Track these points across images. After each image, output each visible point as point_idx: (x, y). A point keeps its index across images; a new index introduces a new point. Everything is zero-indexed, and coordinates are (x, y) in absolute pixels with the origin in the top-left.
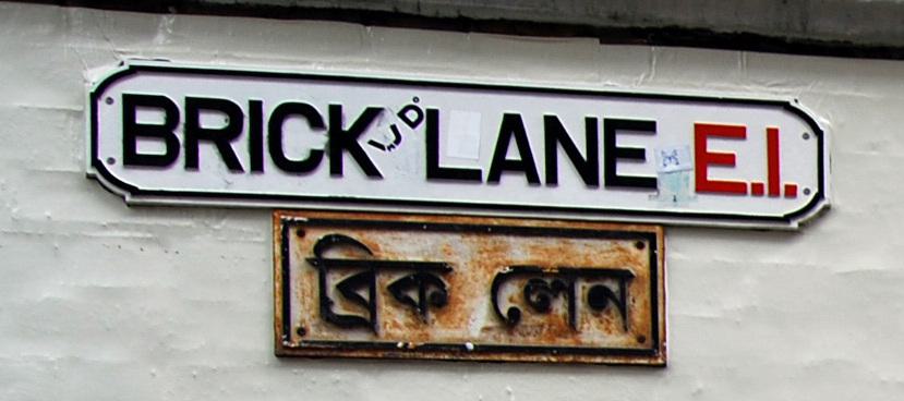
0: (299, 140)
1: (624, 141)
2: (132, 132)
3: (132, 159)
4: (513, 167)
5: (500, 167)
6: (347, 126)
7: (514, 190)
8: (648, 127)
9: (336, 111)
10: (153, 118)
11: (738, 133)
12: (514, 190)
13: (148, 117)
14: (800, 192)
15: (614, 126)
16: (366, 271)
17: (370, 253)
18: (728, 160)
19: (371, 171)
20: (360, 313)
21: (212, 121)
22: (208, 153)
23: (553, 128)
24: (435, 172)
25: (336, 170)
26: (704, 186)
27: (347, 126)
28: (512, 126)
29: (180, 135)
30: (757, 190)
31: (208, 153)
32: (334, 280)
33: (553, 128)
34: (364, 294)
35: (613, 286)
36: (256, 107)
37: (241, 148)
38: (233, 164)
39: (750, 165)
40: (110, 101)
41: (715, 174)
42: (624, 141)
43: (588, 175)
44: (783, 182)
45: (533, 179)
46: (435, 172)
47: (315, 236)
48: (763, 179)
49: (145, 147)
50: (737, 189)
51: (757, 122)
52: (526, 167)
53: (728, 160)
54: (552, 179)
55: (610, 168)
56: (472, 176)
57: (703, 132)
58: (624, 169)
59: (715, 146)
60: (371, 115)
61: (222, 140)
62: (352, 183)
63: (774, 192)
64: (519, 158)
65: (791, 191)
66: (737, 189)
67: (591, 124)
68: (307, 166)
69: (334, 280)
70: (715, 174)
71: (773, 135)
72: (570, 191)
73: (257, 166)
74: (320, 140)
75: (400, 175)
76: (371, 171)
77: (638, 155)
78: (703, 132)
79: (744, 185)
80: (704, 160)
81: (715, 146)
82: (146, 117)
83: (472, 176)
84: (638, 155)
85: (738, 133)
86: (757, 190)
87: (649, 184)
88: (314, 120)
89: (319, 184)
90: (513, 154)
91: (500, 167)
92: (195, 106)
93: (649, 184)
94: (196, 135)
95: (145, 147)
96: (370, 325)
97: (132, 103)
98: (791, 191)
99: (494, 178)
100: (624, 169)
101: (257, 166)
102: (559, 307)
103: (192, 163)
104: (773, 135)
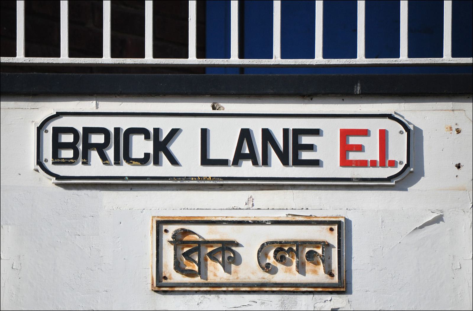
2: (57, 146)
3: (57, 160)
4: (246, 157)
5: (239, 157)
8: (316, 132)
10: (68, 138)
15: (298, 132)
18: (359, 148)
19: (174, 162)
22: (94, 155)
23: (267, 134)
24: (206, 161)
25: (157, 162)
29: (80, 148)
30: (373, 164)
31: (94, 155)
33: (267, 134)
41: (353, 156)
45: (255, 163)
46: (206, 161)
52: (252, 157)
53: (359, 148)
54: (266, 162)
56: (223, 163)
58: (305, 155)
60: (174, 133)
61: (101, 149)
63: (383, 164)
64: (249, 153)
65: (393, 164)
67: (286, 131)
70: (353, 156)
76: (174, 162)
77: (310, 147)
78: (345, 134)
80: (346, 148)
83: (223, 163)
84: (310, 147)
86: (373, 164)
90: (246, 150)
91: (239, 157)
92: (88, 131)
94: (88, 146)
97: (57, 131)
98: (393, 164)
99: (236, 163)
100: (305, 155)
101: (117, 162)
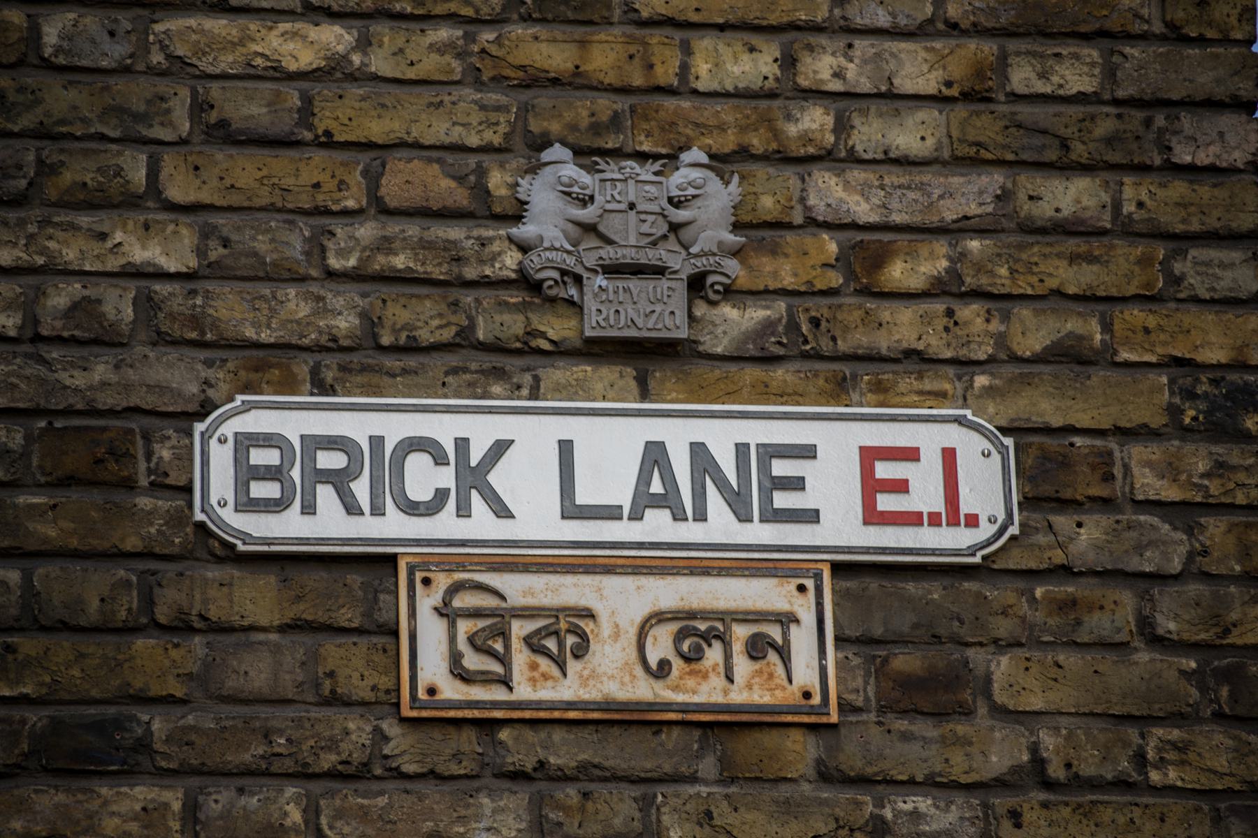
0: (422, 479)
1: (780, 468)
2: (246, 474)
4: (658, 502)
5: (643, 503)
6: (475, 458)
7: (658, 526)
8: (807, 452)
9: (462, 445)
10: (270, 457)
11: (911, 455)
12: (658, 526)
13: (262, 457)
14: (983, 521)
15: (771, 452)
16: (497, 622)
17: (503, 598)
18: (900, 487)
19: (502, 511)
20: (497, 668)
21: (330, 460)
22: (325, 494)
24: (572, 511)
25: (463, 511)
26: (872, 517)
27: (475, 458)
28: (655, 456)
29: (296, 474)
30: (935, 520)
32: (464, 627)
33: (699, 451)
34: (499, 646)
35: (775, 632)
37: (361, 489)
38: (352, 508)
39: (926, 492)
40: (222, 441)
41: (885, 502)
42: (780, 468)
43: (739, 506)
44: (965, 509)
45: (679, 516)
46: (572, 511)
47: (442, 581)
48: (939, 506)
49: (259, 490)
50: (913, 519)
51: (930, 439)
52: (669, 501)
53: (900, 487)
54: (701, 516)
55: (767, 499)
56: (610, 513)
57: (870, 456)
58: (782, 500)
59: (884, 470)
60: (500, 448)
61: (340, 481)
62: (482, 524)
63: (954, 521)
64: (662, 491)
65: (972, 521)
66: (913, 519)
67: (742, 450)
69: (464, 627)
70: (885, 502)
71: (949, 456)
72: (721, 525)
73: (378, 511)
74: (446, 477)
75: (537, 518)
76: (502, 511)
77: (797, 484)
78: (870, 456)
79: (920, 514)
80: (871, 487)
81: (884, 470)
82: (259, 457)
83: (610, 513)
84: (797, 484)
85: (911, 455)
86: (935, 520)
87: (812, 516)
88: (440, 459)
89: (446, 525)
90: (656, 487)
91: (643, 503)
92: (315, 443)
93: (812, 516)
95: (259, 490)
96: (506, 682)
97: (245, 443)
98: (972, 521)
99: (636, 516)
100: (782, 500)
102: (714, 654)
103: (309, 509)
104: (949, 456)
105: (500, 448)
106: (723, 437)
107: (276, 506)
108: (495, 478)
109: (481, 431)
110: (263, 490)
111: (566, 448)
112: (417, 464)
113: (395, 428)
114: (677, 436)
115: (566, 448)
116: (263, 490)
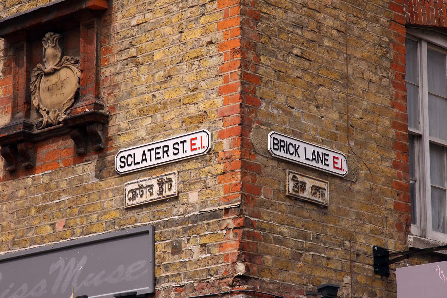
1: (326, 157)
2: (274, 144)
3: (274, 149)
7: (313, 163)
8: (328, 155)
13: (276, 142)
15: (325, 154)
21: (282, 144)
22: (282, 149)
28: (314, 151)
31: (282, 149)
36: (287, 142)
42: (326, 157)
46: (306, 159)
50: (337, 168)
51: (340, 157)
52: (315, 159)
56: (309, 160)
57: (334, 158)
58: (326, 162)
66: (337, 168)
68: (292, 154)
71: (342, 159)
72: (320, 165)
78: (334, 158)
83: (309, 160)
87: (328, 165)
92: (281, 141)
93: (328, 165)
94: (281, 146)
97: (274, 139)
101: (287, 153)
104: (342, 159)
105: (299, 146)
106: (321, 151)
107: (277, 150)
108: (298, 151)
109: (297, 144)
110: (276, 147)
111: (305, 148)
112: (291, 146)
113: (289, 141)
114: (316, 150)
115: (305, 148)
116: (276, 147)
